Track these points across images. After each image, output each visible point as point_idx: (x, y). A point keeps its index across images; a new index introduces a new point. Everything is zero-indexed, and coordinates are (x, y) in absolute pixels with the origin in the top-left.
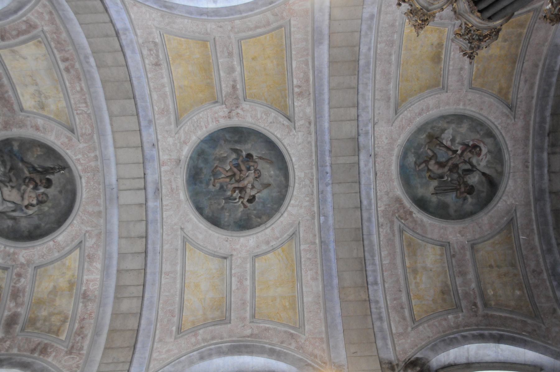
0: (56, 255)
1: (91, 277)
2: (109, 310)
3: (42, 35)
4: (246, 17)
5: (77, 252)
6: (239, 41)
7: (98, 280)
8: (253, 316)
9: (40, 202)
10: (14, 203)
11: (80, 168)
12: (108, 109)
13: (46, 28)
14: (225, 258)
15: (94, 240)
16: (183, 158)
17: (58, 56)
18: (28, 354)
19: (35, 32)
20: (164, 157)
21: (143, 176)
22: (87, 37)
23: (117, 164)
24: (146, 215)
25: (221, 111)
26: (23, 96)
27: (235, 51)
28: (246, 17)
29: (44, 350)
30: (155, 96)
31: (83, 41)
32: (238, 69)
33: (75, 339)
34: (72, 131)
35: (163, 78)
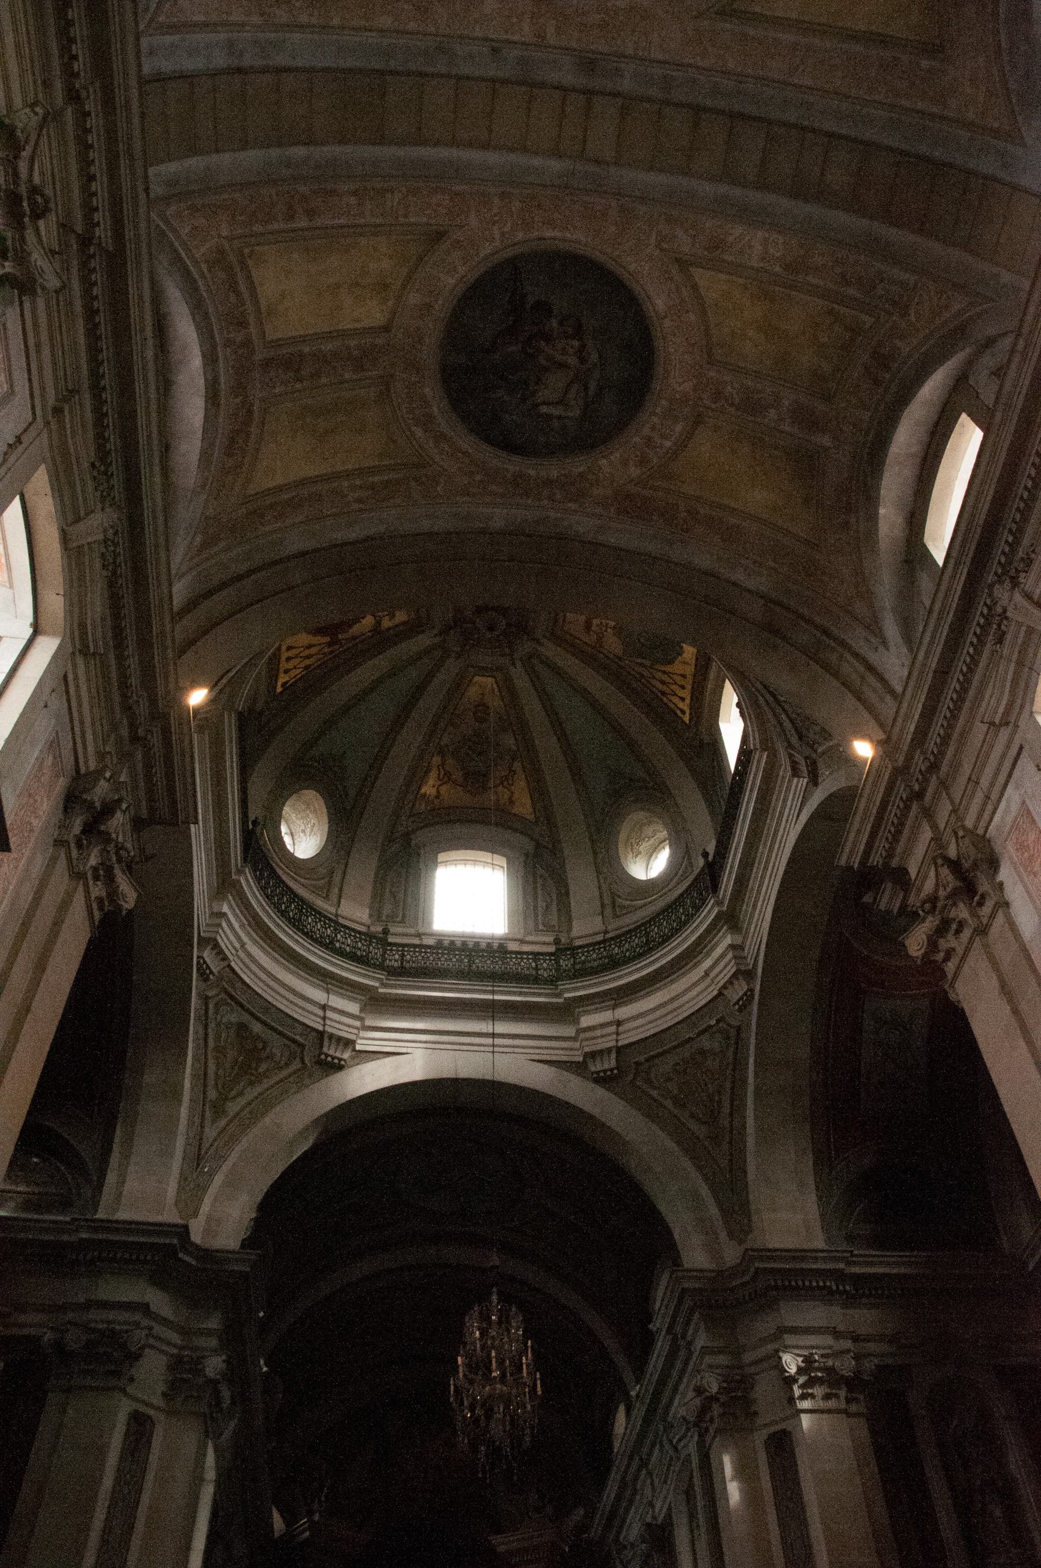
1: (758, 248)
2: (840, 218)
3: (236, 244)
7: (767, 235)
9: (579, 331)
10: (569, 385)
11: (520, 236)
12: (402, 143)
15: (679, 233)
17: (282, 226)
18: (881, 390)
19: (232, 258)
22: (244, 145)
23: (524, 149)
26: (358, 321)
31: (252, 157)
33: (881, 297)
34: (439, 236)
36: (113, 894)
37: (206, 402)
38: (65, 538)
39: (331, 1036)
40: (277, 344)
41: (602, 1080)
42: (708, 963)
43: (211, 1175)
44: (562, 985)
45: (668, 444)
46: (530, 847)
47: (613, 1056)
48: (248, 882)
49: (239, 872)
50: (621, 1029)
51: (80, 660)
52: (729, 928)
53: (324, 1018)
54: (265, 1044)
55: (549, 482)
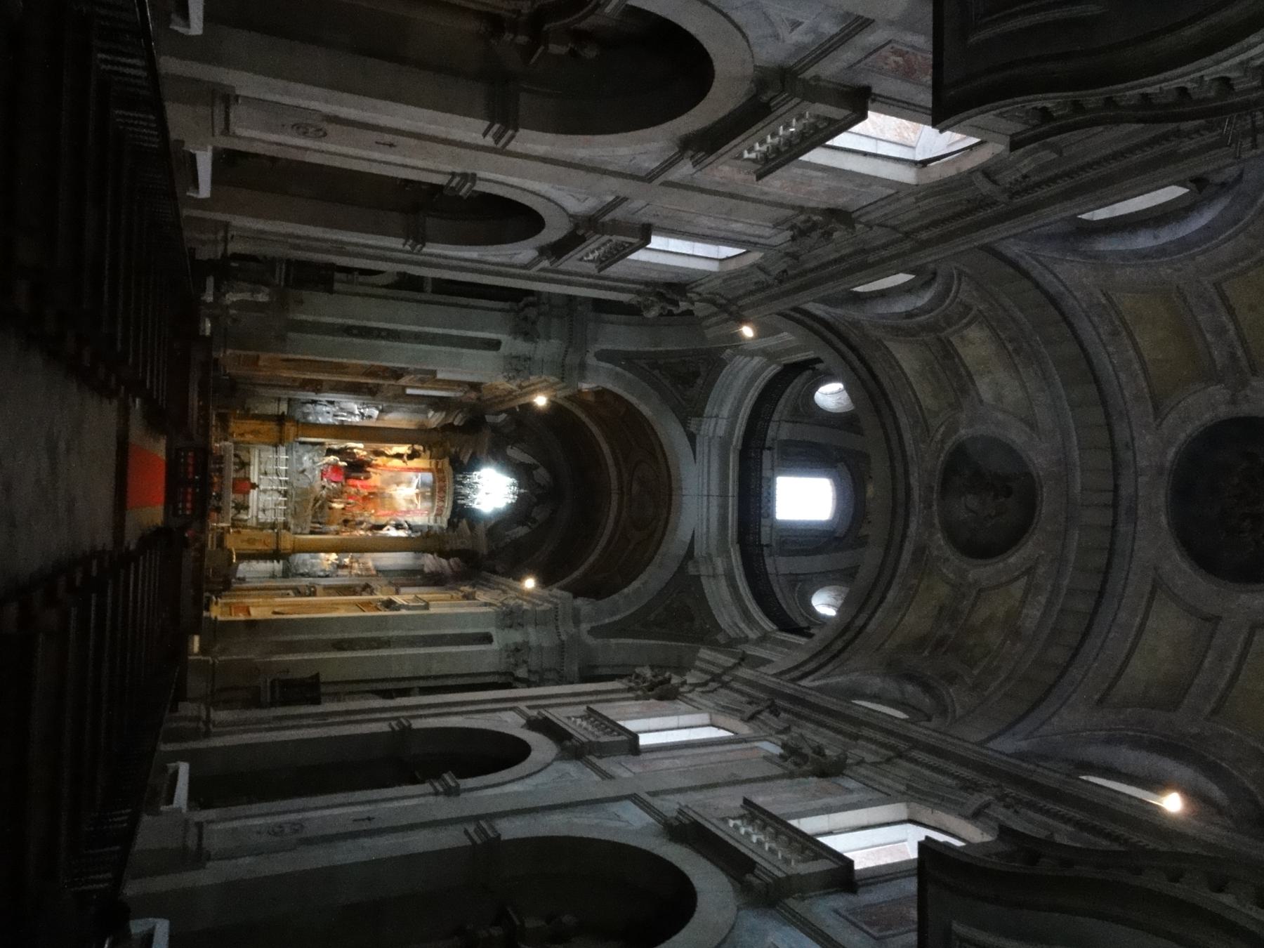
0: (1004, 579)
4: (1207, 250)
5: (1024, 580)
6: (1217, 285)
8: (1215, 712)
13: (981, 307)
14: (1207, 619)
16: (1168, 465)
20: (1143, 463)
21: (1111, 487)
24: (1112, 543)
25: (1218, 393)
27: (1218, 302)
28: (1207, 250)
29: (951, 678)
30: (1123, 376)
32: (1231, 327)
35: (1127, 351)
36: (648, 308)
37: (906, 312)
38: (752, 266)
39: (700, 421)
40: (950, 343)
41: (682, 568)
42: (742, 625)
43: (620, 366)
44: (737, 547)
45: (945, 571)
46: (841, 532)
47: (696, 574)
48: (773, 370)
49: (779, 364)
50: (711, 579)
51: (720, 281)
52: (759, 638)
53: (711, 417)
54: (692, 387)
55: (930, 506)
